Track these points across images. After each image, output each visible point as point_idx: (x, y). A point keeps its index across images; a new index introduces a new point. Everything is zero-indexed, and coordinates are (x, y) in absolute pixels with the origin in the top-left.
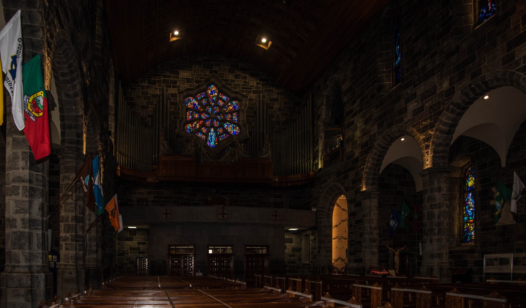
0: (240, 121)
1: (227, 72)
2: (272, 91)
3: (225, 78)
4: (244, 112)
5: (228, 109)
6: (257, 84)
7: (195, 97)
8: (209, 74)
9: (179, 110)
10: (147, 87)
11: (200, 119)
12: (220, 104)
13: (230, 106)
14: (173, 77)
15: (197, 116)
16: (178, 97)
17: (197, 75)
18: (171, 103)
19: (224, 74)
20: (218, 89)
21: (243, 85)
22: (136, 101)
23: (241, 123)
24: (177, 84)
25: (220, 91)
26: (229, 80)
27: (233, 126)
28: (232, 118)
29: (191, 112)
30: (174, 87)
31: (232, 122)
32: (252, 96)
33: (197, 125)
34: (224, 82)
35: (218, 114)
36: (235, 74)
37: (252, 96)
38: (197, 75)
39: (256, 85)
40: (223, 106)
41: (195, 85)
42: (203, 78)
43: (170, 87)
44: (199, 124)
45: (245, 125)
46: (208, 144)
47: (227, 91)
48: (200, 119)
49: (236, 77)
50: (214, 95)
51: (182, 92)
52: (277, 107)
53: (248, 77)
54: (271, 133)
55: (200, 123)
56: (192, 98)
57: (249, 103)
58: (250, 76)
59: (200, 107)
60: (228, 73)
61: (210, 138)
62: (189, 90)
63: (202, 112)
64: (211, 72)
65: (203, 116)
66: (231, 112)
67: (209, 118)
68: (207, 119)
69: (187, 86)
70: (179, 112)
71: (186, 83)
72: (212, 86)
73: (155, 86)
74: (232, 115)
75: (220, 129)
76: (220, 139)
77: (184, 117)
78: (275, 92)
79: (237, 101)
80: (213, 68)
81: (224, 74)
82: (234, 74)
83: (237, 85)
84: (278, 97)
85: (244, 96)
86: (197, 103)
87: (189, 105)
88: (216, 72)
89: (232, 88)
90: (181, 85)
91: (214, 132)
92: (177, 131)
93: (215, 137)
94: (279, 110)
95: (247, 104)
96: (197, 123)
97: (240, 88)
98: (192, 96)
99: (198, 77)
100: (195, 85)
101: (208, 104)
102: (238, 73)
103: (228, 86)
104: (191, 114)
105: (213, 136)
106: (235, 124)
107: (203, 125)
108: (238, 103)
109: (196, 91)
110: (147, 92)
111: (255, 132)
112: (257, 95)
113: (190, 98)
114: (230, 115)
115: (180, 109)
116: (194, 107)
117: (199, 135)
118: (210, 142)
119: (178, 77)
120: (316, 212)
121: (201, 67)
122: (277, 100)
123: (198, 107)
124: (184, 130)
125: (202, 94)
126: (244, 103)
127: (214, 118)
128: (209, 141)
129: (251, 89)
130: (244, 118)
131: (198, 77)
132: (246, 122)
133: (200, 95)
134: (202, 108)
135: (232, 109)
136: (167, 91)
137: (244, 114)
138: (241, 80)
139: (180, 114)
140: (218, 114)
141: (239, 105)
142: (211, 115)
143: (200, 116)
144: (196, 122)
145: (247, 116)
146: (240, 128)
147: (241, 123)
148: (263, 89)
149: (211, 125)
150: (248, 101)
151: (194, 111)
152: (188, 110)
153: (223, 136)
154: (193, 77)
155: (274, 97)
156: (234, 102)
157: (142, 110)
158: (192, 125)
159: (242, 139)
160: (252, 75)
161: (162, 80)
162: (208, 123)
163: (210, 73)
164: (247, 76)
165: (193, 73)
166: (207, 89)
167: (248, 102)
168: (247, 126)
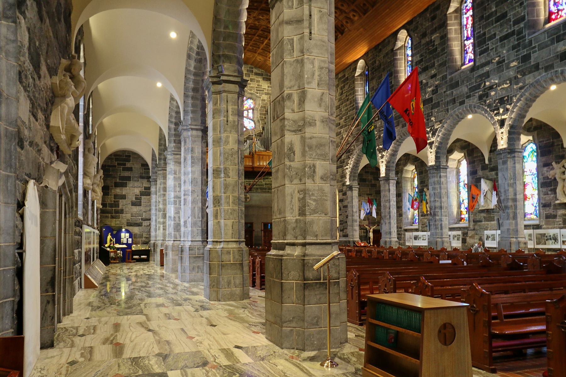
0: (255, 118)
6: (268, 87)
21: (256, 88)
23: (255, 119)
28: (248, 115)
32: (265, 97)
45: (258, 121)
66: (247, 110)
74: (248, 112)
83: (252, 87)
85: (257, 96)
102: (253, 78)
106: (251, 120)
126: (258, 102)
145: (261, 114)
146: (255, 124)
147: (255, 119)
160: (264, 79)
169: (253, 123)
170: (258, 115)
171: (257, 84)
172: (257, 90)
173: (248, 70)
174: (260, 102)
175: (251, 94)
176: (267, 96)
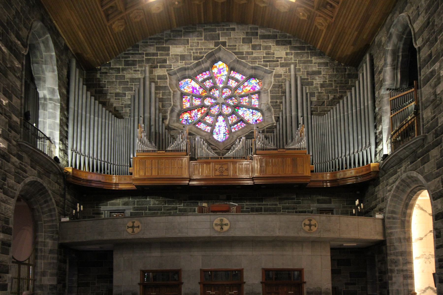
0: (263, 105)
1: (240, 43)
2: (311, 62)
3: (237, 51)
4: (268, 92)
5: (244, 90)
6: (287, 54)
7: (193, 77)
8: (213, 47)
9: (170, 95)
10: (123, 70)
11: (203, 106)
12: (231, 84)
13: (247, 86)
14: (161, 55)
15: (197, 102)
16: (168, 80)
17: (196, 49)
18: (157, 88)
19: (236, 46)
20: (228, 66)
21: (264, 57)
22: (108, 87)
24: (167, 63)
25: (232, 69)
26: (244, 53)
27: (252, 113)
29: (189, 97)
30: (161, 67)
31: (250, 107)
32: (280, 70)
33: (198, 113)
34: (236, 56)
35: (230, 97)
36: (253, 44)
37: (280, 70)
38: (196, 49)
39: (285, 56)
40: (236, 88)
41: (194, 62)
42: (205, 53)
43: (156, 67)
44: (201, 112)
45: (269, 109)
46: (215, 136)
47: (242, 68)
48: (203, 106)
49: (254, 47)
50: (222, 73)
51: (175, 74)
52: (319, 83)
53: (272, 47)
54: (309, 116)
55: (203, 111)
56: (189, 79)
57: (274, 79)
58: (276, 45)
59: (203, 91)
60: (242, 44)
61: (216, 129)
62: (185, 69)
63: (206, 97)
64: (216, 44)
65: (207, 102)
66: (249, 95)
67: (217, 104)
68: (213, 106)
69: (181, 64)
70: (171, 98)
71: (180, 60)
72: (220, 63)
73: (134, 68)
74: (250, 98)
75: (232, 118)
76: (233, 130)
77: (178, 104)
78: (315, 63)
79: (258, 79)
80: (219, 40)
81: (236, 46)
82: (251, 44)
84: (321, 69)
85: (266, 72)
86: (197, 86)
87: (187, 89)
88: (224, 44)
89: (249, 62)
90: (172, 64)
91: (224, 121)
92: (167, 122)
93: (225, 128)
94: (322, 86)
95: (271, 82)
96: (198, 111)
97: (261, 62)
98: (189, 77)
99: (197, 53)
100: (194, 62)
101: (215, 87)
102: (257, 43)
103: (243, 61)
104: (189, 101)
105: (221, 126)
106: (256, 109)
107: (207, 114)
108: (260, 82)
109: (195, 70)
110: (124, 76)
111: (284, 117)
112: (286, 69)
113: (187, 80)
114: (247, 98)
115: (172, 94)
116: (193, 91)
117: (201, 126)
118: (217, 134)
119: (168, 55)
120: (383, 220)
121: (202, 40)
122: (319, 73)
123: (199, 91)
124: (178, 121)
125: (205, 74)
127: (223, 104)
128: (217, 133)
129: (278, 61)
130: (268, 101)
131: (197, 53)
132: (271, 105)
133: (202, 75)
134: (204, 92)
135: (249, 90)
136: (151, 72)
137: (268, 95)
138: (262, 51)
139: (172, 101)
140: (230, 97)
141: (261, 84)
142: (218, 99)
143: (202, 102)
144: (196, 110)
145: (272, 98)
148: (296, 60)
149: (219, 112)
150: (274, 77)
151: (193, 96)
152: (184, 95)
153: (238, 126)
154: (190, 52)
155: (314, 69)
156: (253, 82)
157: (115, 99)
158: (190, 114)
159: (265, 128)
160: (278, 43)
161: (144, 59)
162: (214, 111)
163: (215, 46)
164: (270, 46)
165: (189, 48)
166: (212, 66)
167: (273, 78)
168: (273, 110)
169: (259, 114)
170: (267, 99)
171: (265, 51)
172: (264, 61)
173: (247, 33)
174: (271, 80)
175: (255, 68)
176: (284, 69)
